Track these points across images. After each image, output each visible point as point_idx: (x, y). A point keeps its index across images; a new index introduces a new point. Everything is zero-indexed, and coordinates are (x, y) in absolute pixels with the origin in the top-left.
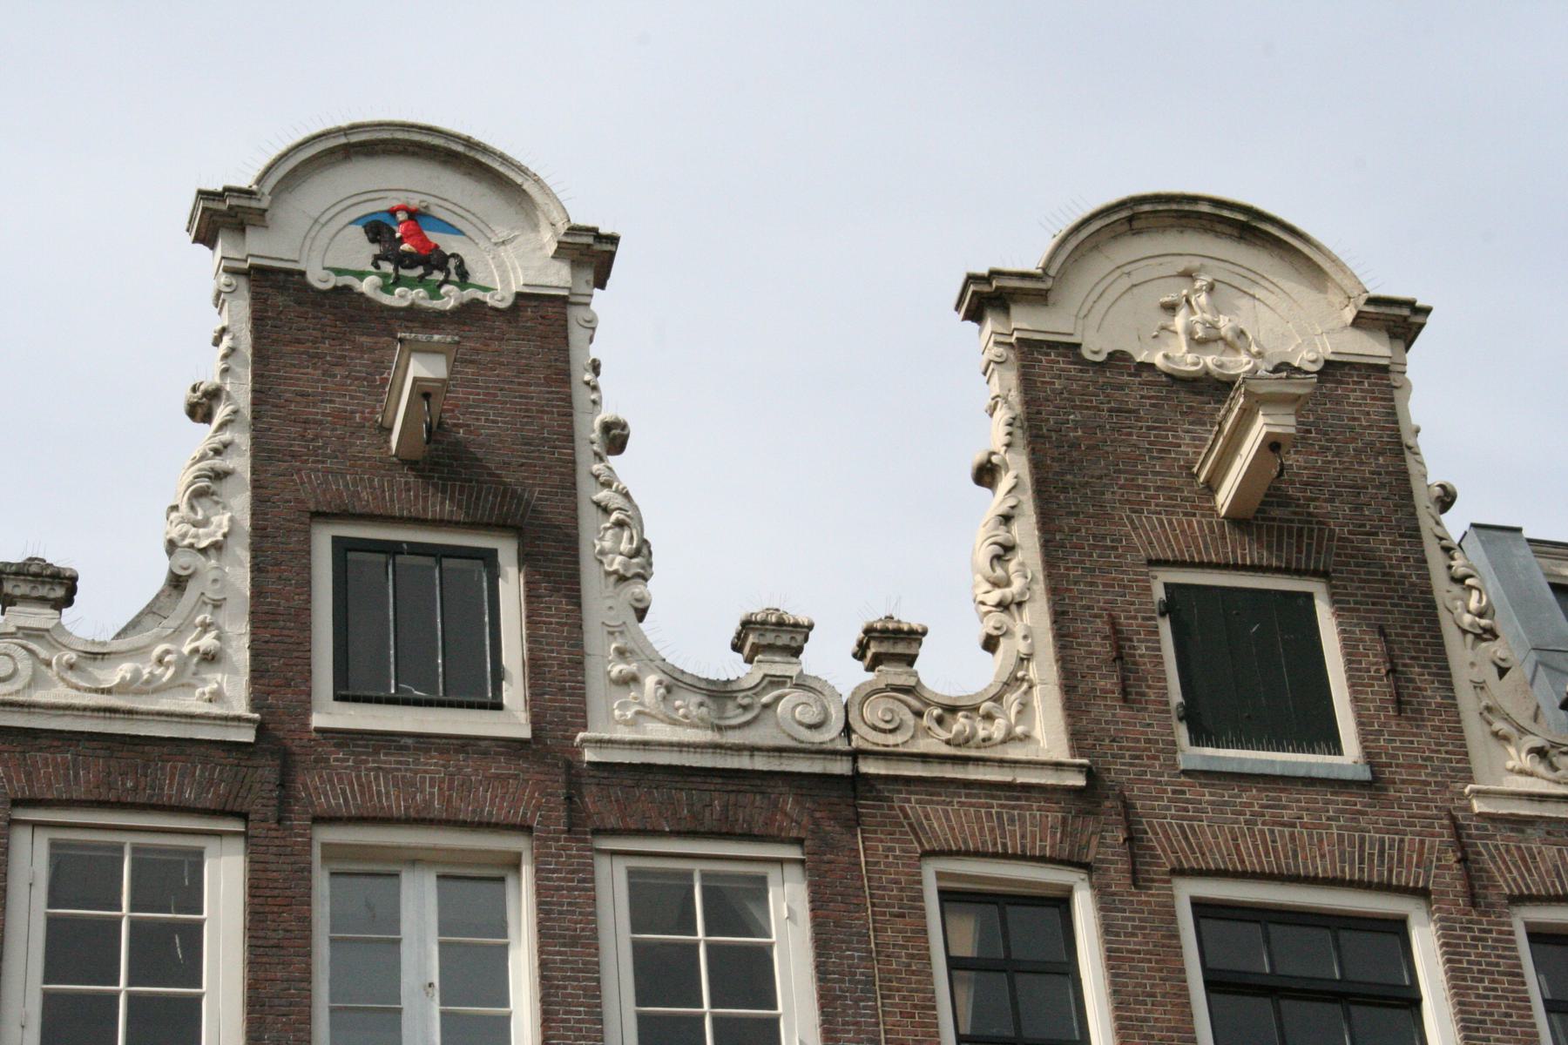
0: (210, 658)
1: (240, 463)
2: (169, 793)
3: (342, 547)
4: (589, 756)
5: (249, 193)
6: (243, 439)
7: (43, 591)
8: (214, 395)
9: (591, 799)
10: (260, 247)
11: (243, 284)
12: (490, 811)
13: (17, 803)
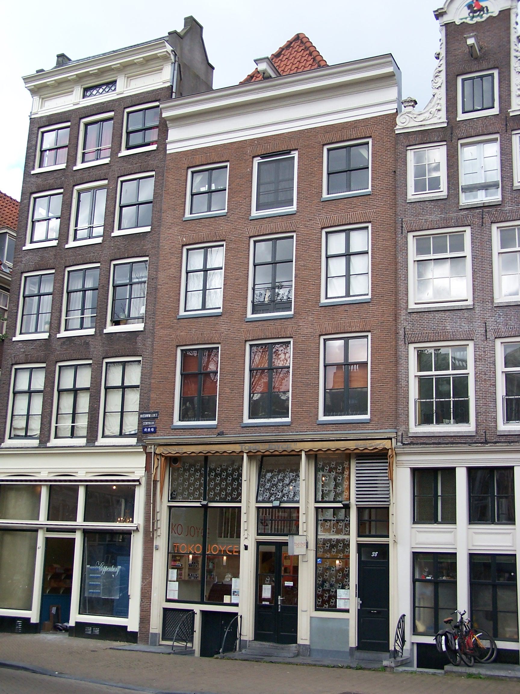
0: (439, 110)
1: (443, 68)
2: (432, 140)
3: (464, 80)
4: (511, 114)
5: (442, 9)
6: (443, 62)
7: (410, 104)
8: (439, 54)
9: (511, 124)
10: (446, 19)
11: (444, 27)
12: (491, 131)
13: (407, 146)
